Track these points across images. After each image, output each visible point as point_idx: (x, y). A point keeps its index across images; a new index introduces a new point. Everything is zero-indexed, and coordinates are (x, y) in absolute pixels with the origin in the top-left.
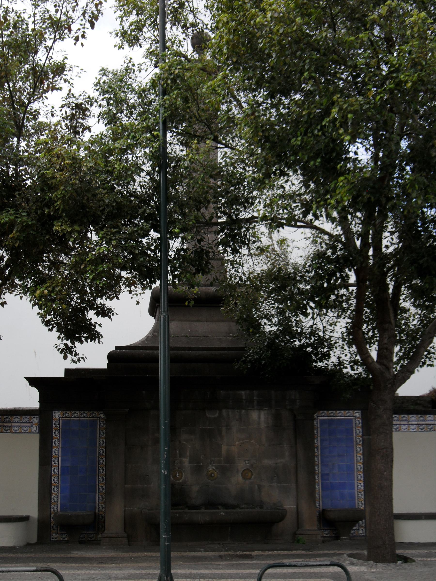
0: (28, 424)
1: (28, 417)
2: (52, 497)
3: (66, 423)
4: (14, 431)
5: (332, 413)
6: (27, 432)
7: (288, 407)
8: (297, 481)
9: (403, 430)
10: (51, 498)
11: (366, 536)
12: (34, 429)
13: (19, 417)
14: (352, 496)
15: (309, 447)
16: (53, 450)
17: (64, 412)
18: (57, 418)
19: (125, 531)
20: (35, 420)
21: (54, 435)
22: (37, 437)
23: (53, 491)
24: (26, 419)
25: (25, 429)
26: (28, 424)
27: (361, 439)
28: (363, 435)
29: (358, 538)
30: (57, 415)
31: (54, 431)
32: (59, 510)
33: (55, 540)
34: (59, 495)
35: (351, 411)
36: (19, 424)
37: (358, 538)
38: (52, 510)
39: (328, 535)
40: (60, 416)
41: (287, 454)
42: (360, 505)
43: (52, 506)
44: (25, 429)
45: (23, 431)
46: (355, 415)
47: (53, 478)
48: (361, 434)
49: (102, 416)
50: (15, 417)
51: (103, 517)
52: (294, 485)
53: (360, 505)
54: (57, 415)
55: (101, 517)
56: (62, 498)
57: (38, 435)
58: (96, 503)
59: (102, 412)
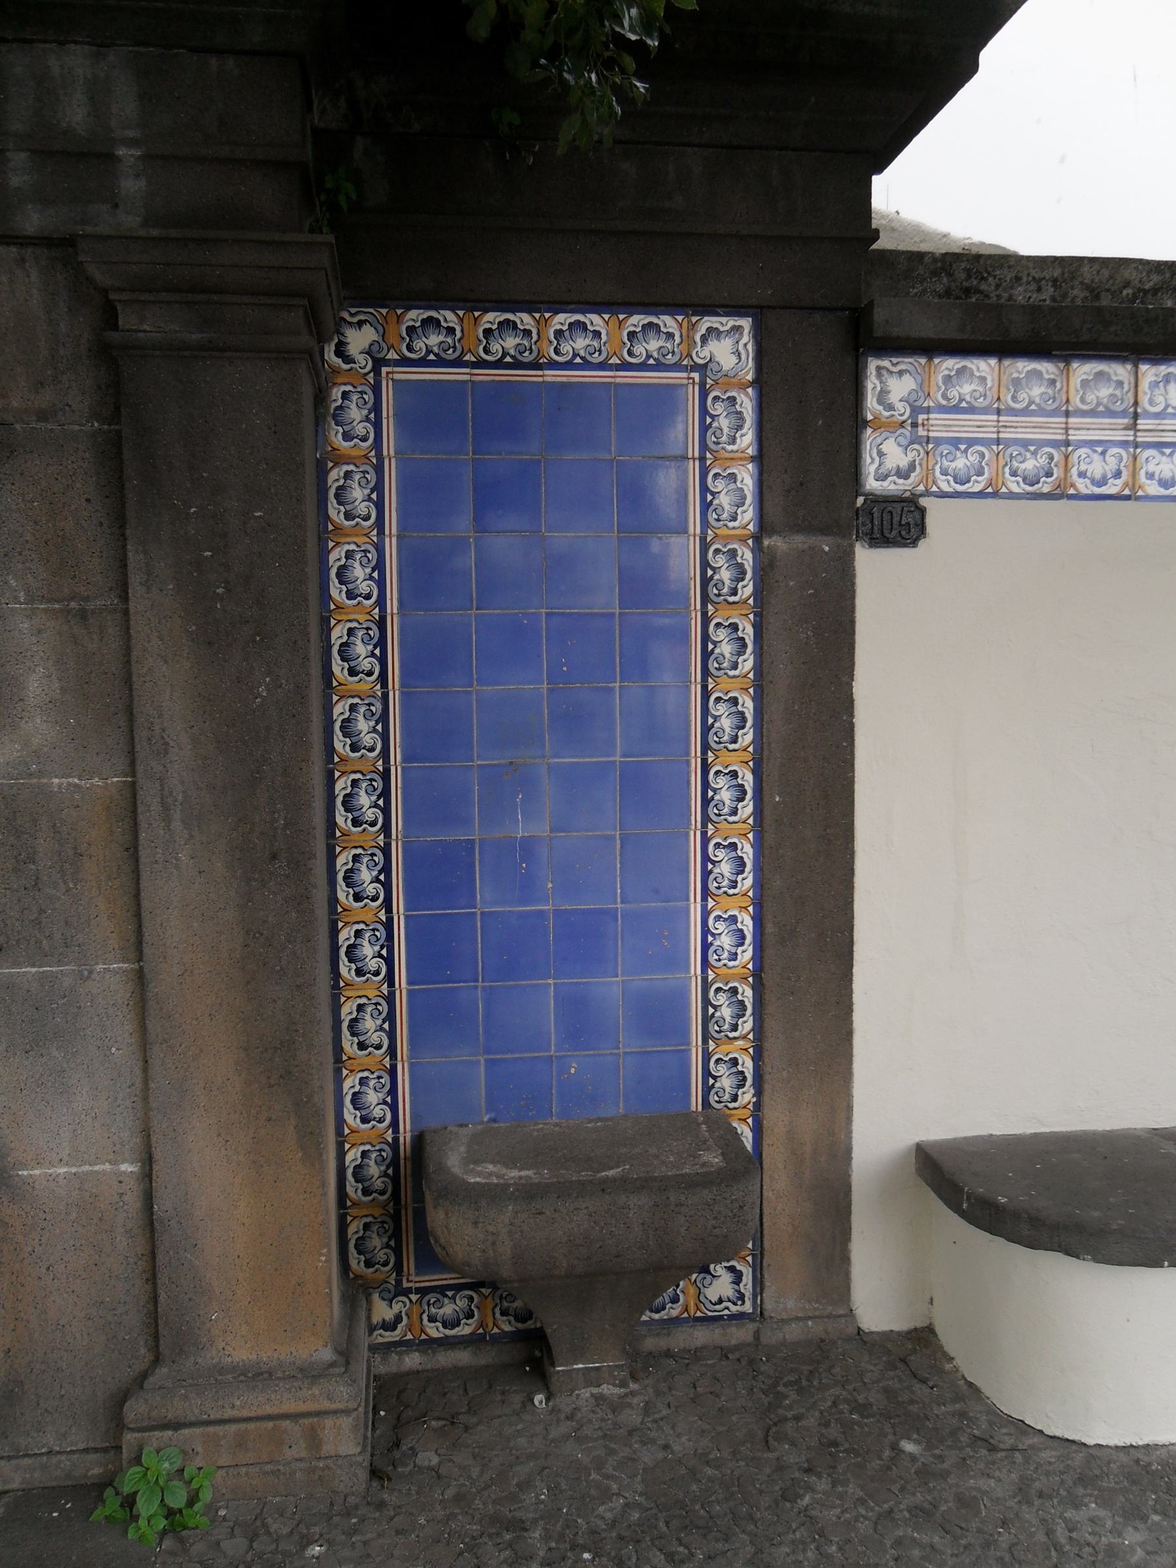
5: (507, 332)
7: (32, 221)
8: (137, 946)
9: (1084, 487)
11: (760, 1315)
14: (660, 1017)
15: (261, 611)
27: (747, 557)
28: (764, 526)
29: (701, 1336)
35: (668, 322)
37: (701, 1336)
39: (464, 1330)
41: (38, 684)
42: (726, 1083)
46: (701, 354)
48: (748, 515)
52: (110, 974)
53: (726, 1083)
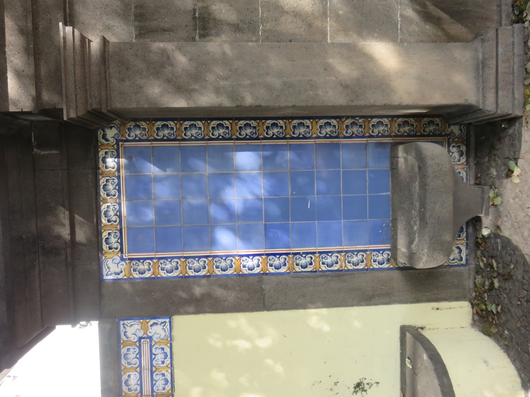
0: (146, 348)
1: (124, 351)
2: (350, 267)
3: (137, 238)
4: (168, 387)
6: (167, 350)
10: (354, 270)
12: (157, 330)
13: (125, 377)
16: (218, 272)
17: (105, 247)
18: (123, 266)
19: (470, 41)
20: (132, 329)
21: (175, 274)
22: (183, 323)
23: (336, 267)
24: (132, 355)
25: (160, 357)
26: (146, 348)
30: (113, 268)
31: (163, 274)
32: (388, 246)
33: (464, 256)
34: (346, 248)
36: (146, 375)
38: (385, 266)
40: (118, 259)
43: (375, 266)
44: (160, 357)
45: (167, 361)
47: (298, 269)
49: (111, 133)
50: (125, 388)
51: (406, 123)
54: (114, 268)
55: (407, 128)
56: (352, 240)
57: (177, 319)
58: (366, 145)
59: (100, 133)
